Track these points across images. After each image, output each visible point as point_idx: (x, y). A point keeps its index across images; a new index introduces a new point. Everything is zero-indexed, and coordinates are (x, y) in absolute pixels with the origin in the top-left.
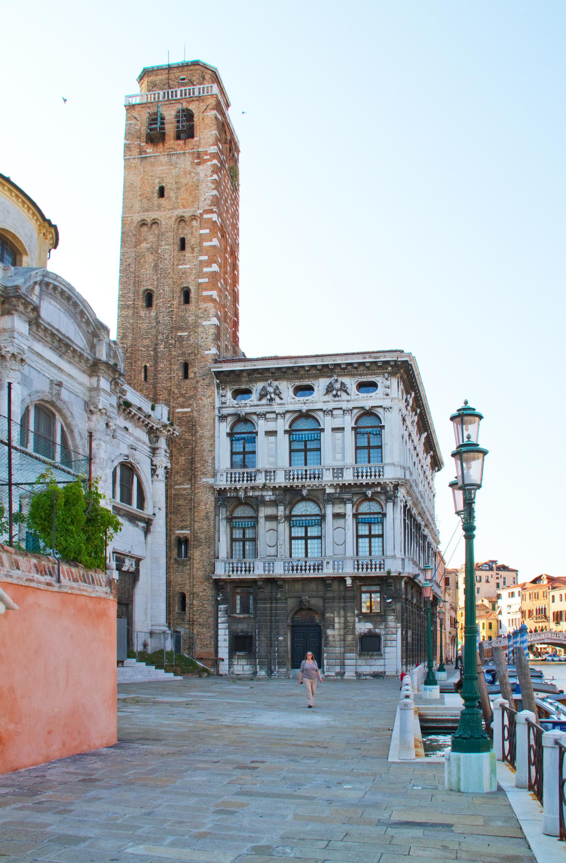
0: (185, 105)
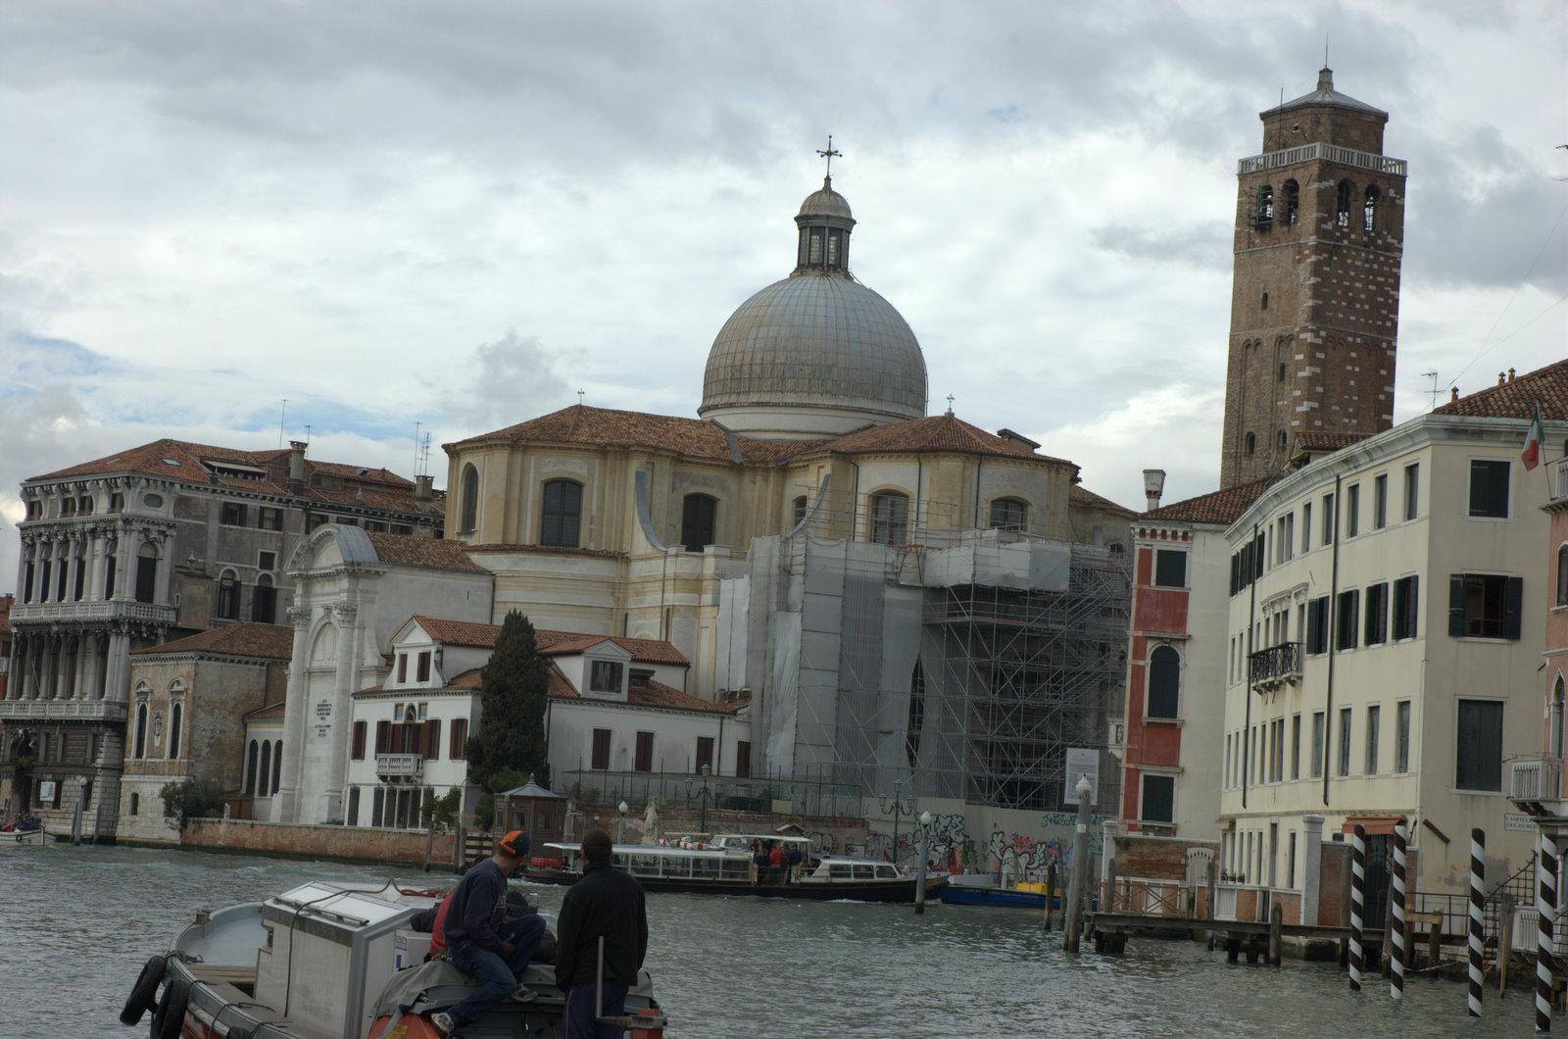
0: (1288, 175)
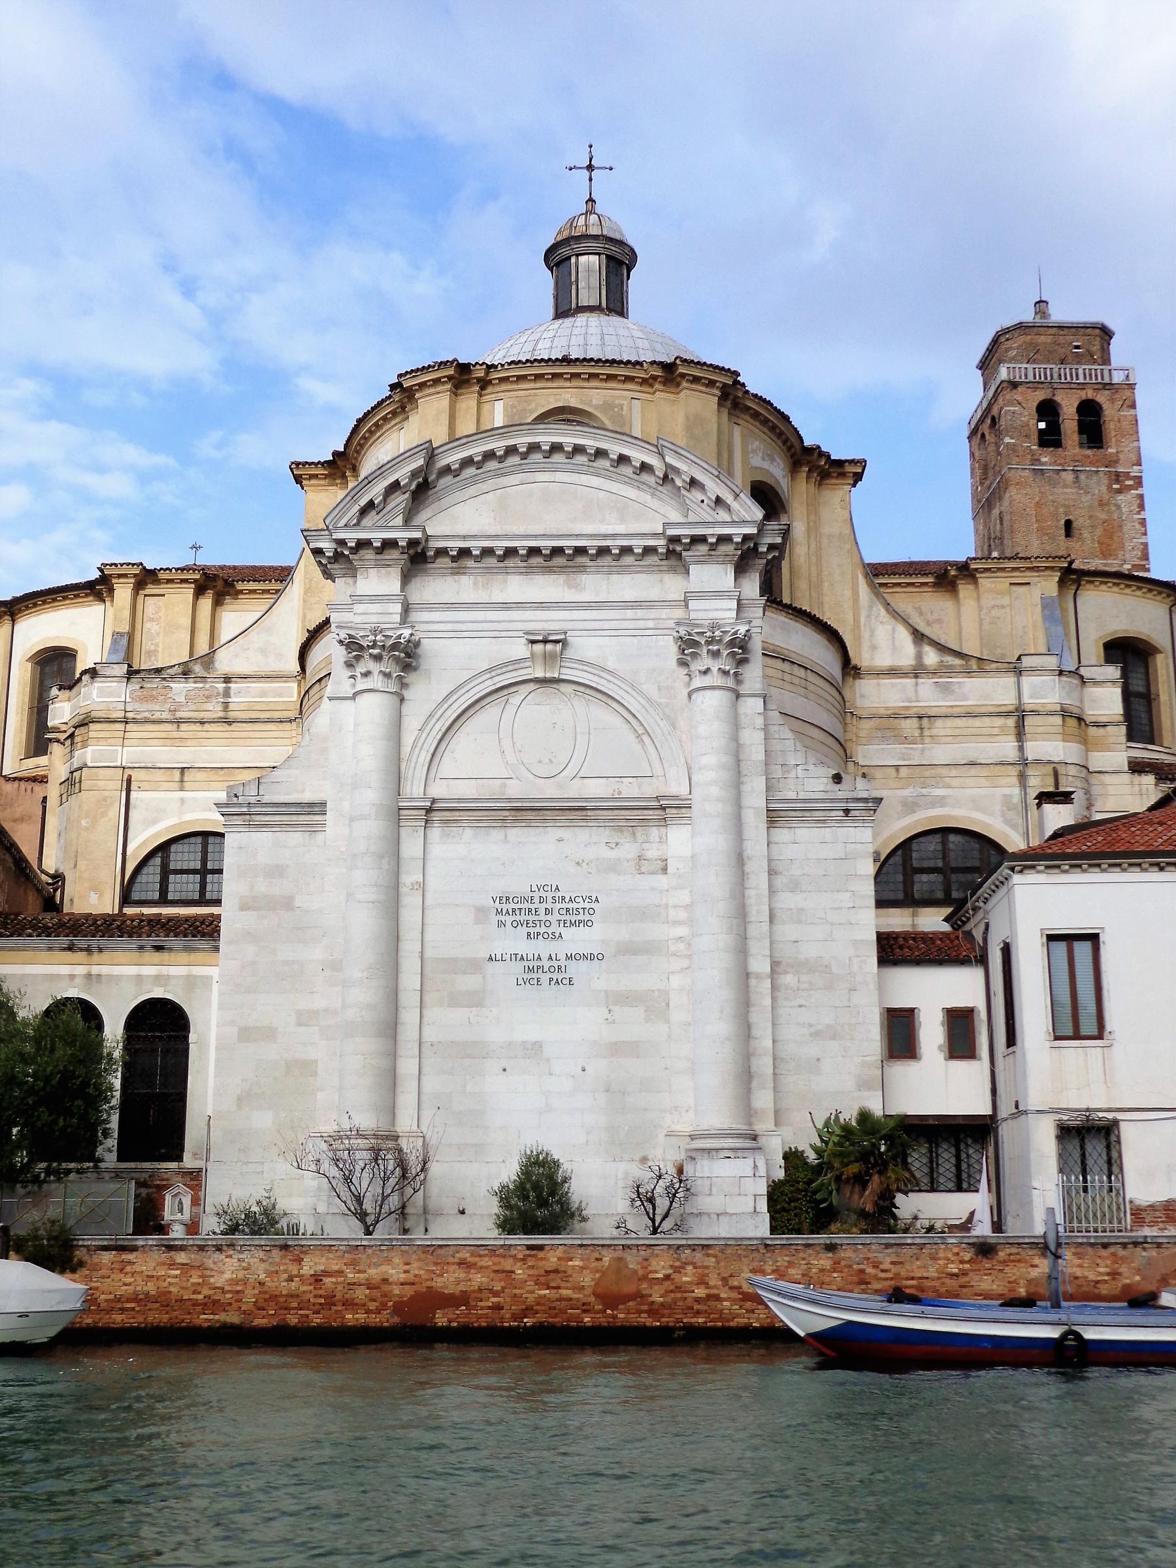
0: (1090, 394)
